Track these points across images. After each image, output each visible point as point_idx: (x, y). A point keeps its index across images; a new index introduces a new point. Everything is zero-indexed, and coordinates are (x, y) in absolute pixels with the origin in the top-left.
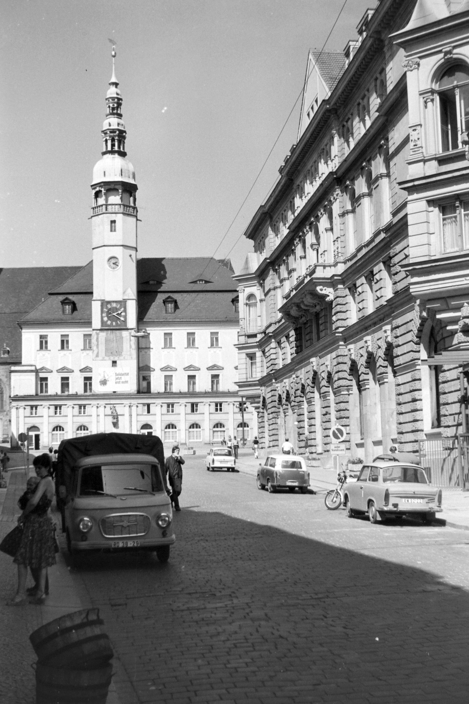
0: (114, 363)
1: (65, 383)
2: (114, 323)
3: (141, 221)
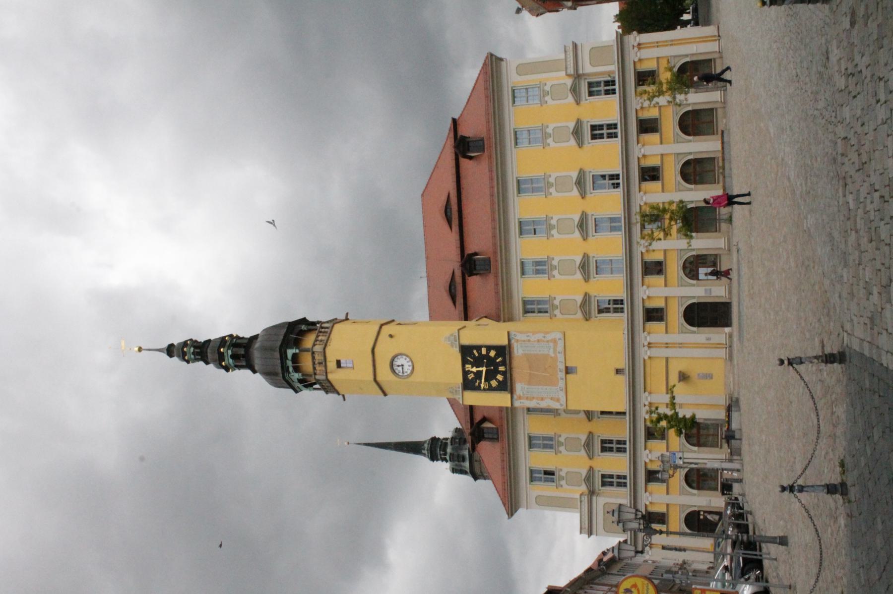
0: (568, 370)
2: (502, 368)
3: (347, 314)
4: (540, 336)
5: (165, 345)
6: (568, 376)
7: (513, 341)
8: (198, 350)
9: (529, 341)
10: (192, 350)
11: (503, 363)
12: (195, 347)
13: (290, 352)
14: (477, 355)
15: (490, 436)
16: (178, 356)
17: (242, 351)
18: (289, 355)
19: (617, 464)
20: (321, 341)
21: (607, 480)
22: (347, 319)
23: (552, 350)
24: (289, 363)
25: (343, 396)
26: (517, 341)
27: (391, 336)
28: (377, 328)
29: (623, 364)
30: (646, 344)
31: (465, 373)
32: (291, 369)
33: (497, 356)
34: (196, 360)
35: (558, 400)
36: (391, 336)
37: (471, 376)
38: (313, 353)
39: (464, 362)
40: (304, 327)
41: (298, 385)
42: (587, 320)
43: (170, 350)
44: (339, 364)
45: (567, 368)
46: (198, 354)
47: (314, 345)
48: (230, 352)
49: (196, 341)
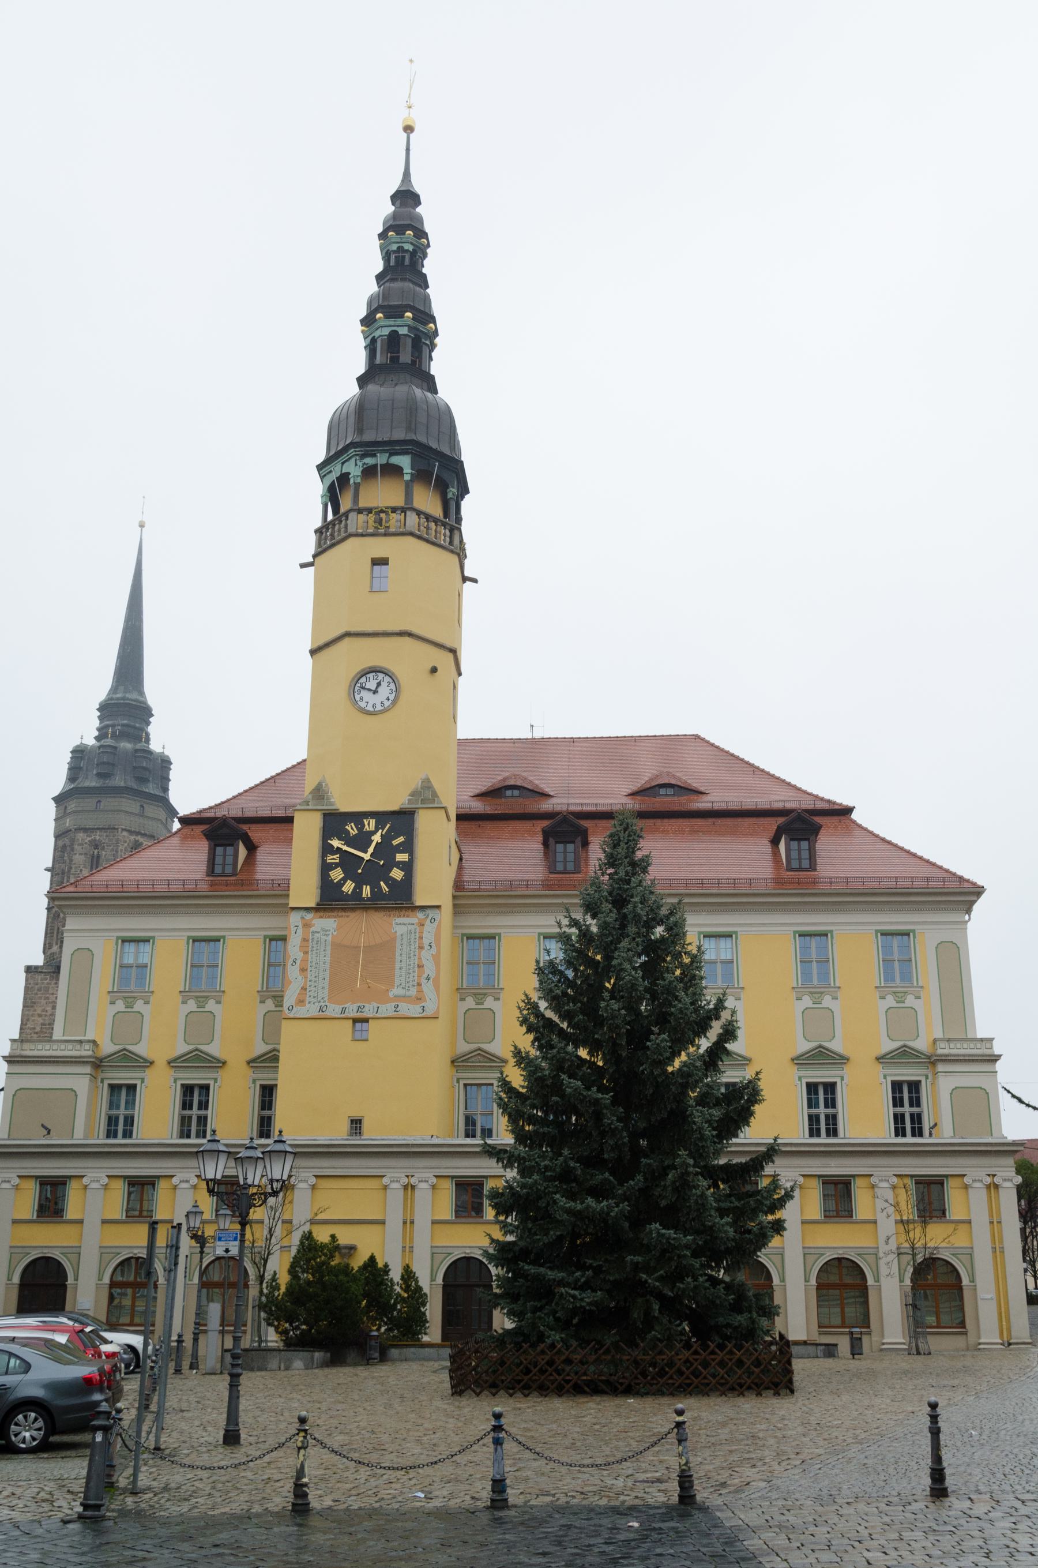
1: (194, 1098)
2: (366, 891)
3: (475, 581)
4: (429, 969)
5: (418, 186)
6: (351, 1021)
7: (420, 915)
8: (407, 262)
9: (421, 948)
10: (409, 247)
11: (377, 894)
12: (413, 254)
13: (404, 462)
14: (395, 842)
15: (219, 860)
16: (395, 216)
17: (406, 357)
18: (396, 460)
19: (157, 1118)
20: (428, 528)
21: (123, 1093)
22: (465, 579)
23: (400, 992)
24: (381, 459)
25: (311, 564)
27: (434, 670)
29: (371, 1134)
30: (413, 1181)
31: (358, 817)
32: (370, 461)
33: (392, 883)
34: (386, 256)
35: (301, 1002)
36: (434, 670)
37: (352, 829)
38: (404, 510)
39: (381, 817)
40: (452, 491)
41: (336, 471)
42: (453, 1062)
43: (406, 197)
44: (380, 562)
45: (366, 1020)
46: (400, 261)
47: (419, 513)
48: (403, 331)
49: (425, 256)
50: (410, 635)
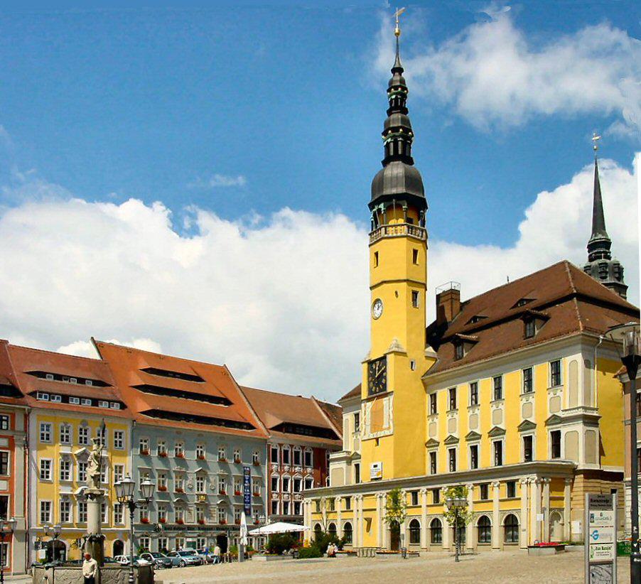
0: (377, 439)
13: (382, 206)
26: (389, 399)
28: (405, 278)
50: (385, 282)
